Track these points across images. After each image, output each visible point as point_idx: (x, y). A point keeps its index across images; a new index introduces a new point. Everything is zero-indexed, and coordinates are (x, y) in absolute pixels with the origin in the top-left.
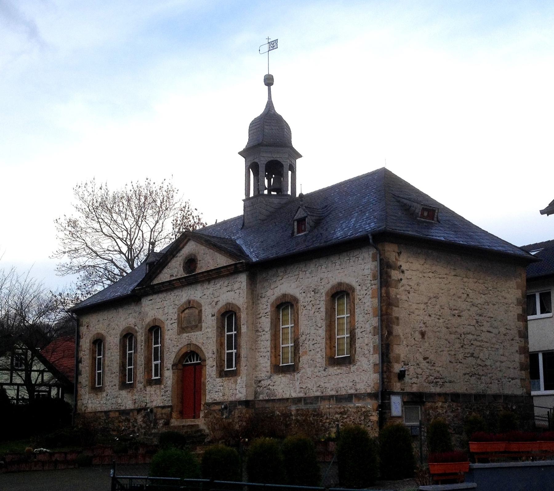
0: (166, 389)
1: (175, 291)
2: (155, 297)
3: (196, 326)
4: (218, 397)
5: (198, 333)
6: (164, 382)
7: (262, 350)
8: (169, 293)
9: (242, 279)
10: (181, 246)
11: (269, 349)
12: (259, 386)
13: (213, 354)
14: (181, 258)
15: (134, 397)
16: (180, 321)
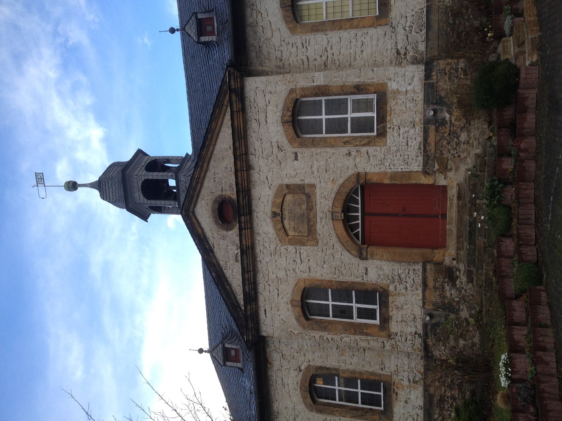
0: (397, 278)
1: (258, 251)
2: (261, 298)
3: (308, 196)
4: (416, 136)
5: (318, 191)
6: (385, 282)
7: (352, 51)
8: (260, 266)
9: (253, 85)
10: (200, 231)
11: (353, 32)
12: (405, 54)
13: (349, 154)
14: (215, 235)
15: (406, 383)
16: (298, 242)
